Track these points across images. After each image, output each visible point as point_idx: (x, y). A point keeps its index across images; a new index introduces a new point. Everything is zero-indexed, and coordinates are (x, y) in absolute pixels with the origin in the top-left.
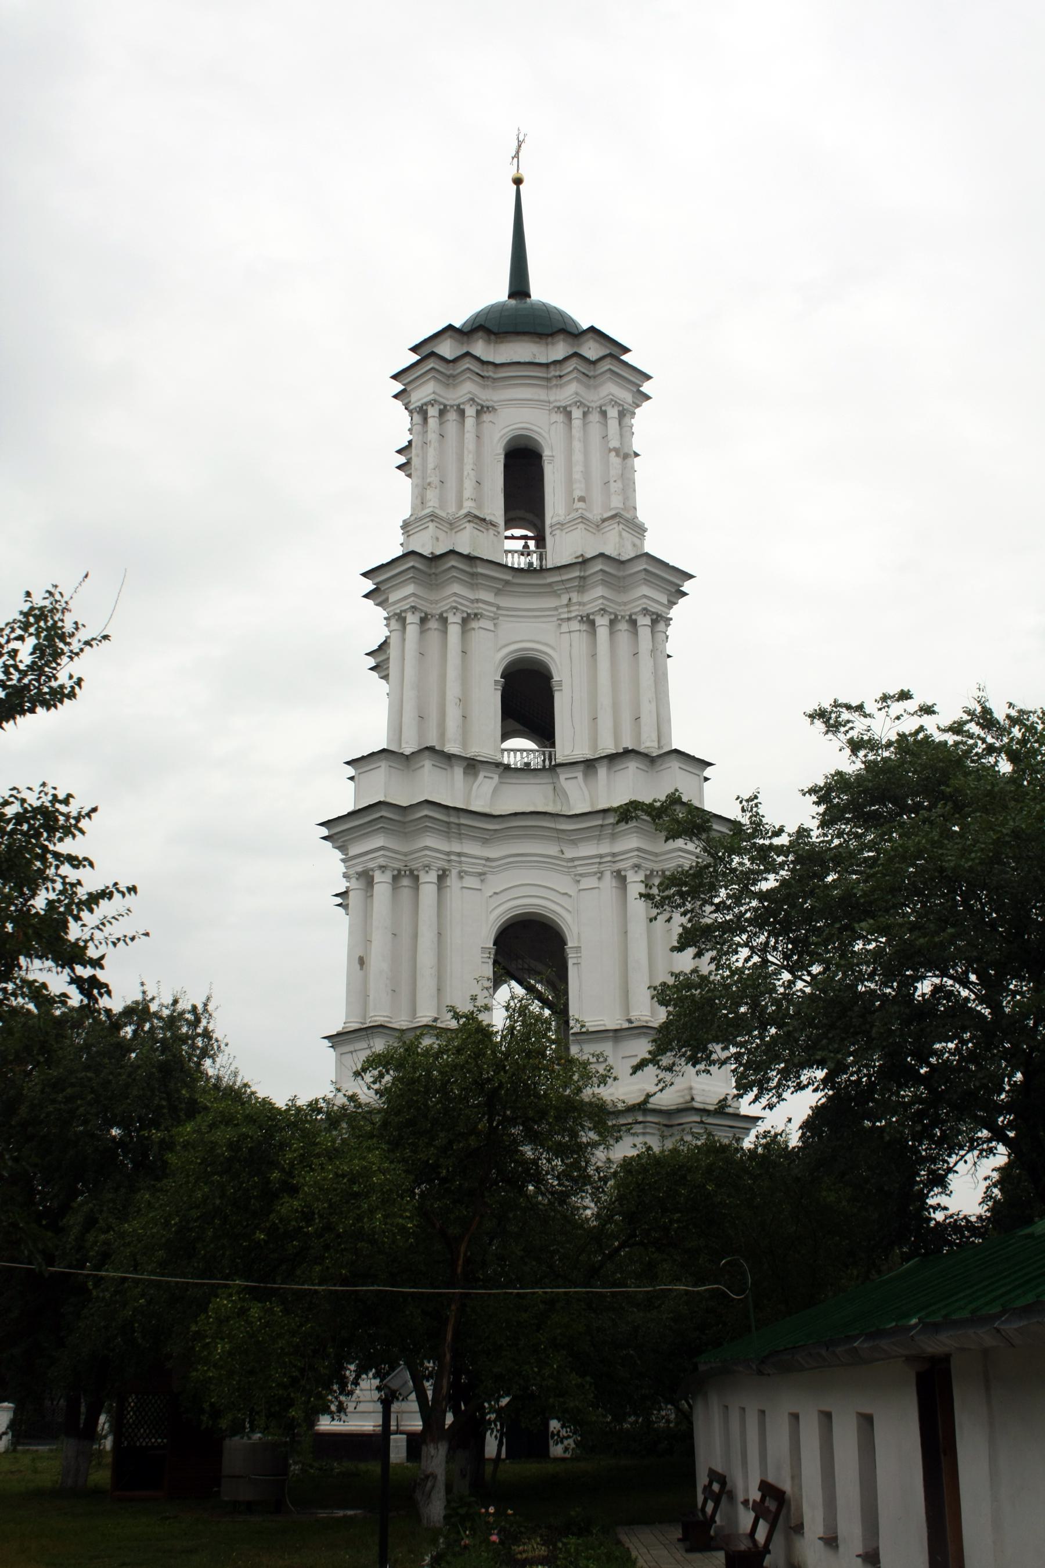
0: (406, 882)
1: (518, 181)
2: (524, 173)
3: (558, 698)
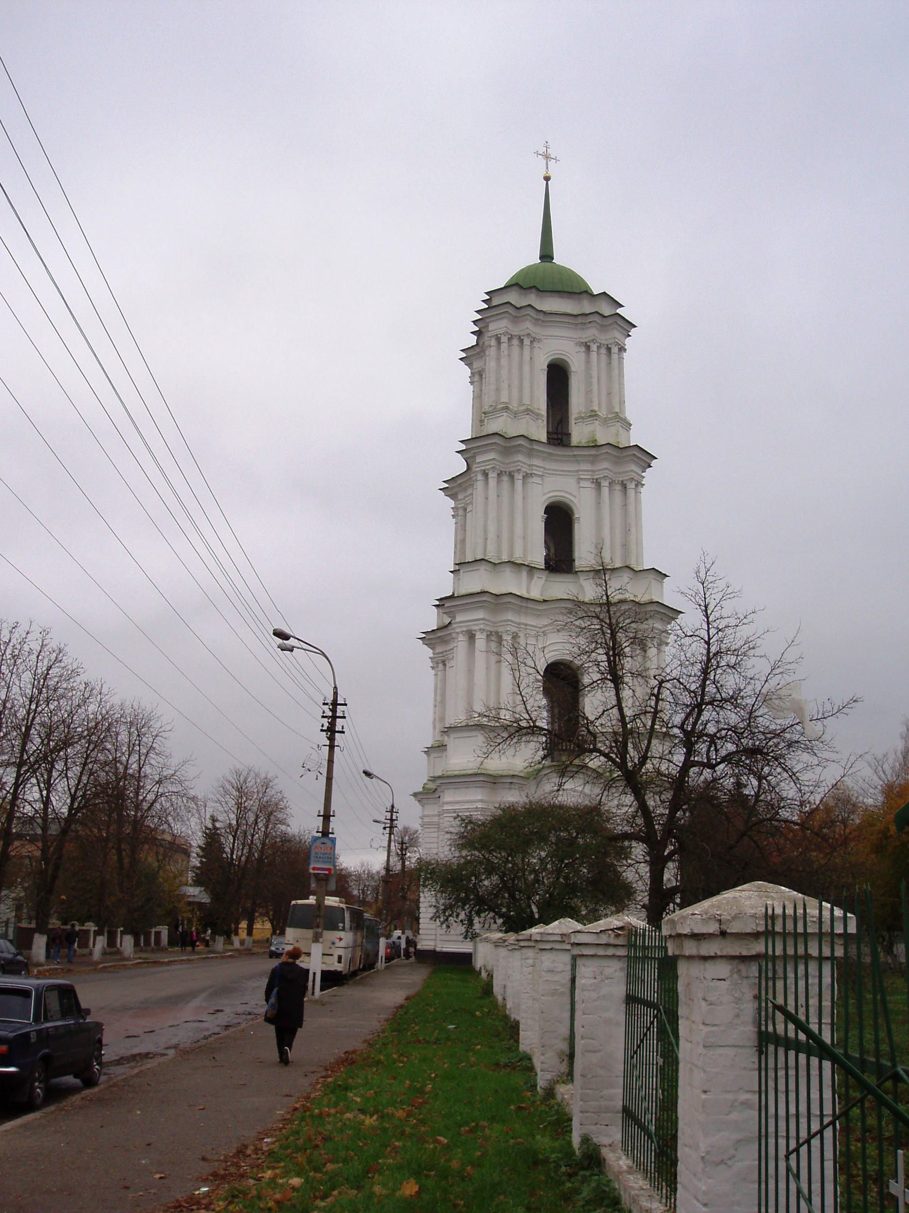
0: (493, 638)
1: (547, 179)
2: (550, 173)
3: (577, 527)
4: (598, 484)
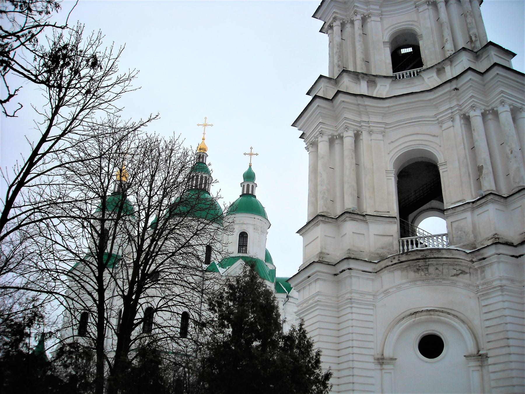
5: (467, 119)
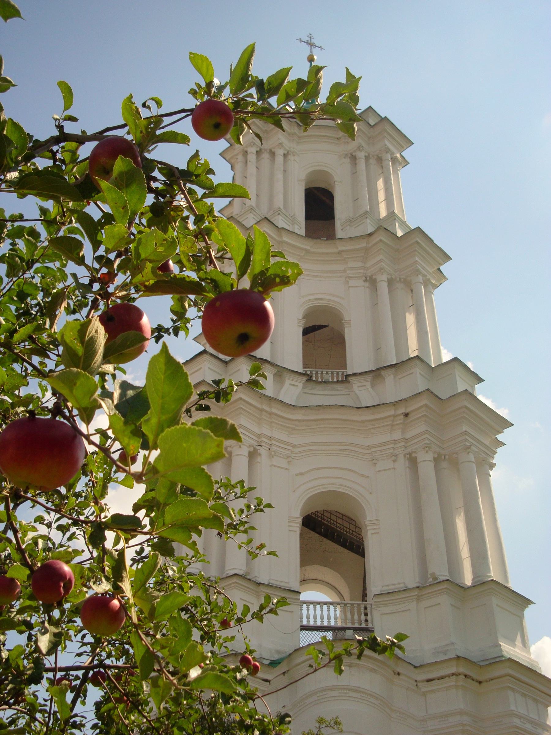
4: (372, 282)
5: (413, 462)
